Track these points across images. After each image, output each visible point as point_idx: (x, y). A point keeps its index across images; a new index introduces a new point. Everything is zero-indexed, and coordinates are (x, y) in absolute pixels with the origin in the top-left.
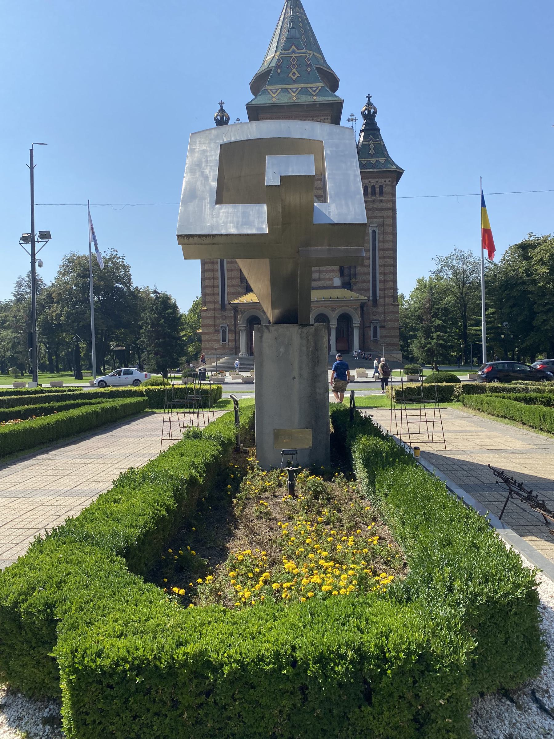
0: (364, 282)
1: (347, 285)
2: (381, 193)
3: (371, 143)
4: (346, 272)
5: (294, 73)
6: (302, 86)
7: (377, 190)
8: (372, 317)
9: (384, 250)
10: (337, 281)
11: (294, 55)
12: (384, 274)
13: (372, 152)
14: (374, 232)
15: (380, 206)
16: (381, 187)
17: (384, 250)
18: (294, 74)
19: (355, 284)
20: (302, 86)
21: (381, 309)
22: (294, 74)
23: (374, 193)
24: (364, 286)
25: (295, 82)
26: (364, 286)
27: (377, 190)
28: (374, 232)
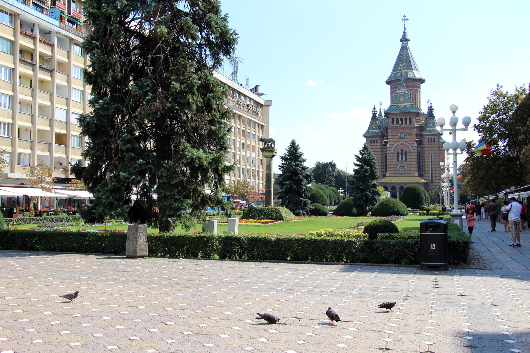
0: (428, 174)
1: (421, 175)
2: (434, 141)
3: (431, 122)
4: (421, 170)
5: (402, 99)
6: (404, 104)
7: (433, 140)
8: (431, 187)
9: (435, 162)
10: (417, 174)
11: (402, 91)
12: (435, 171)
13: (431, 125)
14: (432, 155)
15: (434, 146)
16: (434, 139)
17: (435, 162)
18: (402, 99)
19: (424, 174)
20: (404, 104)
21: (434, 184)
22: (402, 99)
23: (431, 141)
24: (428, 175)
25: (402, 103)
26: (428, 175)
27: (433, 140)
28: (432, 155)
